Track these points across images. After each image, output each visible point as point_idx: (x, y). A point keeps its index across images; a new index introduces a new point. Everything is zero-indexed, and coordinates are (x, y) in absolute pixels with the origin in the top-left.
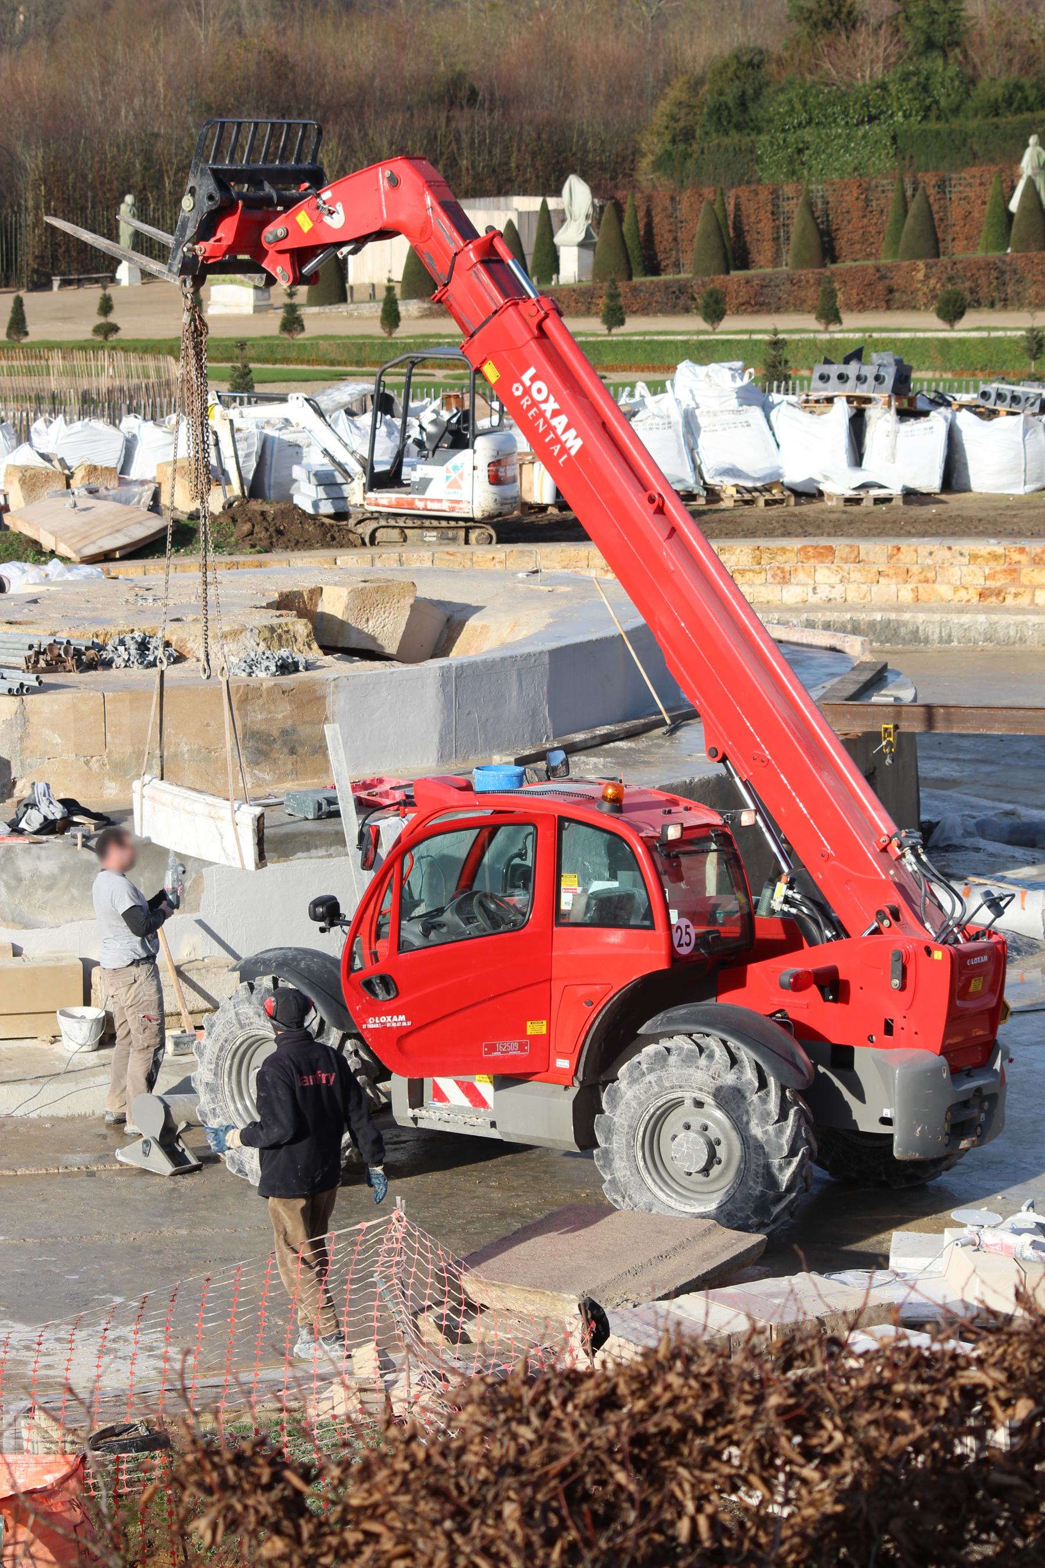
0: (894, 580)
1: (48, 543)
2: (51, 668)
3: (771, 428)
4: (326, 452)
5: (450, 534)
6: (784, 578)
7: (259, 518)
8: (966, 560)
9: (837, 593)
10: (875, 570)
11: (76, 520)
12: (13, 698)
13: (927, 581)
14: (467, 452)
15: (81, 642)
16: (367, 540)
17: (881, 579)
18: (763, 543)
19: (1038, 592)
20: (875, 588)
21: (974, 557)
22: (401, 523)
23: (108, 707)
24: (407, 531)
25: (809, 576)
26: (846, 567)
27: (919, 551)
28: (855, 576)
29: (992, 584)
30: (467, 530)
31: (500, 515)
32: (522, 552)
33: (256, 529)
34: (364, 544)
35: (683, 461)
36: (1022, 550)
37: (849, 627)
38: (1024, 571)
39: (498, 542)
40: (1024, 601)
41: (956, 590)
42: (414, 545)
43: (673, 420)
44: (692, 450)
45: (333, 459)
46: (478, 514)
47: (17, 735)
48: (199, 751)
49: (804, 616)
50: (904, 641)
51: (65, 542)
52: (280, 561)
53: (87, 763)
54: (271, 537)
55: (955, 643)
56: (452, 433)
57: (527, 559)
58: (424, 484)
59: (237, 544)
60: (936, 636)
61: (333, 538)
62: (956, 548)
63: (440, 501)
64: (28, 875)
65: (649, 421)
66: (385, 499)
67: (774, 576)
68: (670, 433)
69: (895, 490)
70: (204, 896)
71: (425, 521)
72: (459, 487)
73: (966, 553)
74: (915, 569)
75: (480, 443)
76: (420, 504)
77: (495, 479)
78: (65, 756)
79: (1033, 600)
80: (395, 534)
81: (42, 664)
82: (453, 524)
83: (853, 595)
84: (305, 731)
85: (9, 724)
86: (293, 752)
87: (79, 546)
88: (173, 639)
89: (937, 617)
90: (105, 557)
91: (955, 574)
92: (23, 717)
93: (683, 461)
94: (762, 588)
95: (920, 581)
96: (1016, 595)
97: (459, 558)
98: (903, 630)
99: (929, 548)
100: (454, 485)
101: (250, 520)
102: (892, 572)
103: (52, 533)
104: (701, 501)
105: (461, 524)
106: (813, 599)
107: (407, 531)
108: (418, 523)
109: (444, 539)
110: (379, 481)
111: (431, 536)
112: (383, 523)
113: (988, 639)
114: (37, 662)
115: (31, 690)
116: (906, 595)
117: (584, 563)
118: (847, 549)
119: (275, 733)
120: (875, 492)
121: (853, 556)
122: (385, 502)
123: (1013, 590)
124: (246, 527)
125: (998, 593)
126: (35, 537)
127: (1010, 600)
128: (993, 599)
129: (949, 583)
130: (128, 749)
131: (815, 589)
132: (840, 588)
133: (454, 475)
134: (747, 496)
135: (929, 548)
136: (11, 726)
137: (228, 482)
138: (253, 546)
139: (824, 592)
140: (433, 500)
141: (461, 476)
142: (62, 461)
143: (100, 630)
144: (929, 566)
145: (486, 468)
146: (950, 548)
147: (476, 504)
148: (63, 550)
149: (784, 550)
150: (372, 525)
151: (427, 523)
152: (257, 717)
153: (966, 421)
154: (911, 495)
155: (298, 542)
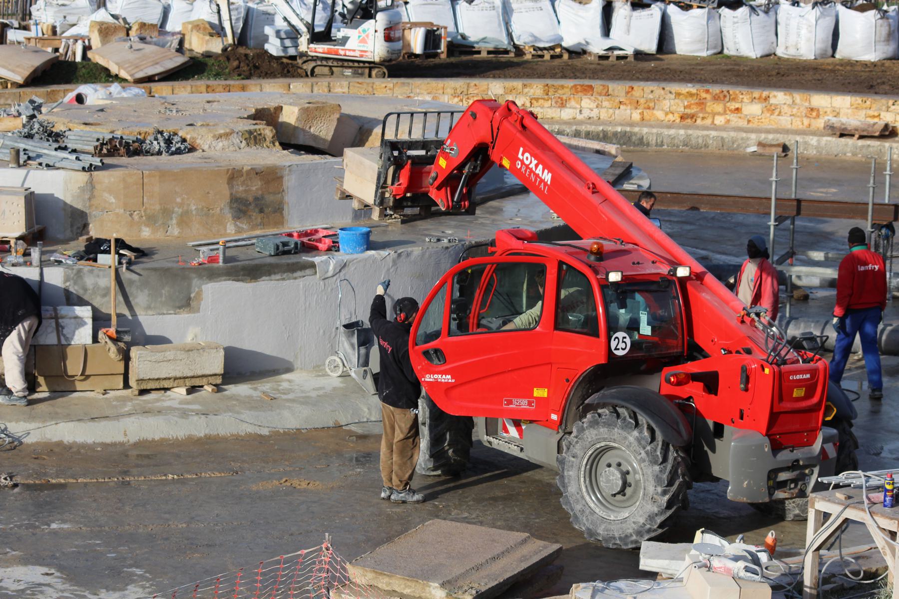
0: (629, 107)
1: (114, 69)
2: (110, 154)
3: (555, 12)
4: (285, 19)
5: (360, 71)
6: (562, 104)
7: (244, 58)
8: (673, 96)
9: (594, 114)
10: (617, 101)
11: (131, 56)
12: (85, 173)
13: (649, 108)
14: (372, 21)
15: (129, 138)
16: (309, 73)
17: (622, 107)
18: (550, 82)
19: (717, 117)
20: (617, 112)
21: (678, 94)
22: (330, 64)
23: (145, 180)
24: (334, 69)
25: (577, 103)
26: (600, 98)
27: (645, 90)
28: (605, 104)
29: (688, 111)
30: (370, 69)
31: (390, 60)
32: (404, 83)
33: (242, 65)
34: (307, 76)
35: (501, 30)
36: (707, 91)
37: (601, 135)
38: (708, 104)
39: (389, 77)
40: (708, 122)
41: (667, 114)
42: (338, 77)
43: (496, 5)
44: (507, 24)
45: (289, 23)
46: (377, 59)
47: (87, 197)
48: (202, 209)
49: (574, 128)
50: (635, 145)
51: (125, 69)
52: (255, 85)
53: (131, 215)
54: (250, 70)
55: (665, 147)
56: (363, 9)
57: (406, 88)
58: (345, 40)
59: (229, 73)
60: (654, 142)
61: (288, 72)
62: (667, 89)
63: (354, 51)
64: (91, 287)
65: (482, 5)
66: (320, 49)
67: (556, 103)
68: (494, 13)
69: (630, 51)
70: (202, 303)
71: (344, 63)
72: (366, 43)
73: (673, 91)
74: (642, 101)
75: (380, 16)
76: (342, 53)
77: (388, 38)
78: (117, 211)
79: (713, 122)
80: (326, 70)
81: (105, 151)
82: (361, 65)
83: (604, 115)
84: (270, 198)
85: (82, 189)
86: (261, 211)
87: (133, 72)
88: (188, 137)
89: (655, 131)
90: (150, 79)
91: (666, 104)
92: (91, 185)
93: (501, 30)
94: (549, 110)
95: (645, 108)
96: (703, 118)
97: (365, 86)
98: (634, 138)
99: (651, 88)
100: (363, 41)
101: (238, 59)
102: (628, 102)
103: (117, 64)
104: (512, 55)
105: (367, 65)
106: (580, 117)
107: (334, 69)
108: (340, 64)
109: (356, 74)
110: (316, 38)
111: (348, 72)
112: (319, 63)
113: (686, 145)
114: (101, 150)
115: (97, 168)
116: (636, 116)
117: (441, 92)
118: (601, 87)
119: (251, 199)
120: (617, 53)
121: (604, 91)
122: (321, 50)
123: (701, 115)
124: (236, 63)
125: (692, 116)
126: (106, 66)
127: (699, 121)
128: (689, 120)
129: (662, 110)
130: (158, 207)
131: (581, 111)
132: (596, 111)
133: (363, 35)
134: (540, 53)
135: (651, 88)
136: (84, 190)
137: (225, 35)
138: (239, 75)
139: (586, 113)
140: (350, 50)
141: (367, 36)
142: (124, 19)
143: (143, 130)
144: (651, 99)
145: (383, 32)
147: (376, 53)
148: (123, 74)
149: (563, 87)
150: (312, 64)
151: (346, 64)
152: (240, 189)
153: (672, 9)
154: (639, 55)
155: (266, 74)
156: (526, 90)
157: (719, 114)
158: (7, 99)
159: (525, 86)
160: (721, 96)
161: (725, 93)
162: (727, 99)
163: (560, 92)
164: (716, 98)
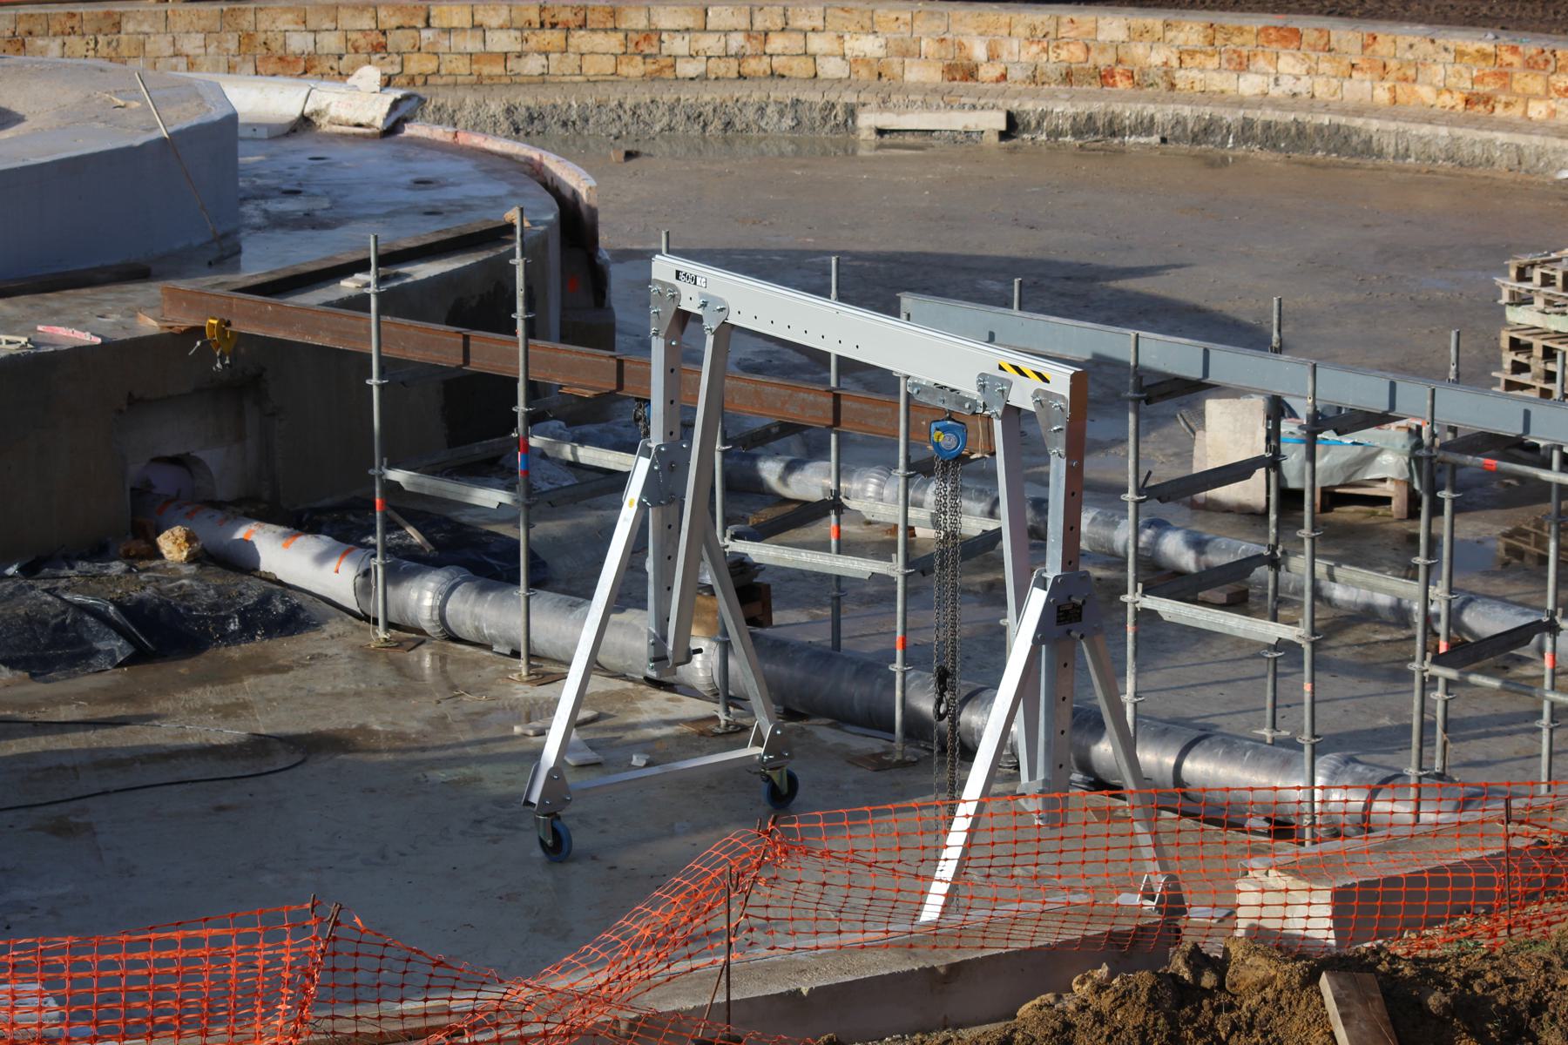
0: (1368, 76)
6: (1242, 65)
8: (1450, 57)
9: (1303, 87)
10: (1346, 62)
13: (1406, 80)
17: (1354, 74)
19: (1532, 104)
20: (1346, 84)
21: (1460, 54)
25: (1270, 63)
26: (1314, 56)
28: (1324, 67)
29: (1479, 88)
36: (1514, 50)
37: (1293, 130)
38: (1517, 76)
40: (1516, 112)
41: (1439, 93)
49: (1241, 113)
50: (1355, 153)
55: (1412, 160)
57: (937, 22)
60: (1391, 149)
62: (1383, 47)
67: (1229, 61)
73: (1451, 47)
74: (1392, 64)
79: (1525, 112)
83: (1321, 90)
89: (1392, 126)
91: (1438, 73)
94: (1216, 75)
95: (1398, 79)
96: (1507, 105)
97: (856, 16)
98: (1355, 139)
99: (1410, 39)
102: (1366, 66)
106: (1274, 92)
113: (1451, 158)
116: (1382, 95)
117: (1005, 32)
118: (1316, 34)
121: (1322, 42)
123: (1503, 98)
125: (1487, 100)
127: (1499, 110)
128: (1480, 108)
129: (1431, 84)
131: (1276, 80)
132: (1305, 79)
135: (1410, 39)
139: (1287, 85)
144: (1409, 61)
146: (1433, 41)
149: (1241, 30)
156: (1170, 35)
157: (1536, 97)
158: (140, 23)
159: (1167, 25)
160: (1540, 60)
161: (1548, 54)
162: (1551, 68)
163: (1236, 40)
164: (1530, 65)
